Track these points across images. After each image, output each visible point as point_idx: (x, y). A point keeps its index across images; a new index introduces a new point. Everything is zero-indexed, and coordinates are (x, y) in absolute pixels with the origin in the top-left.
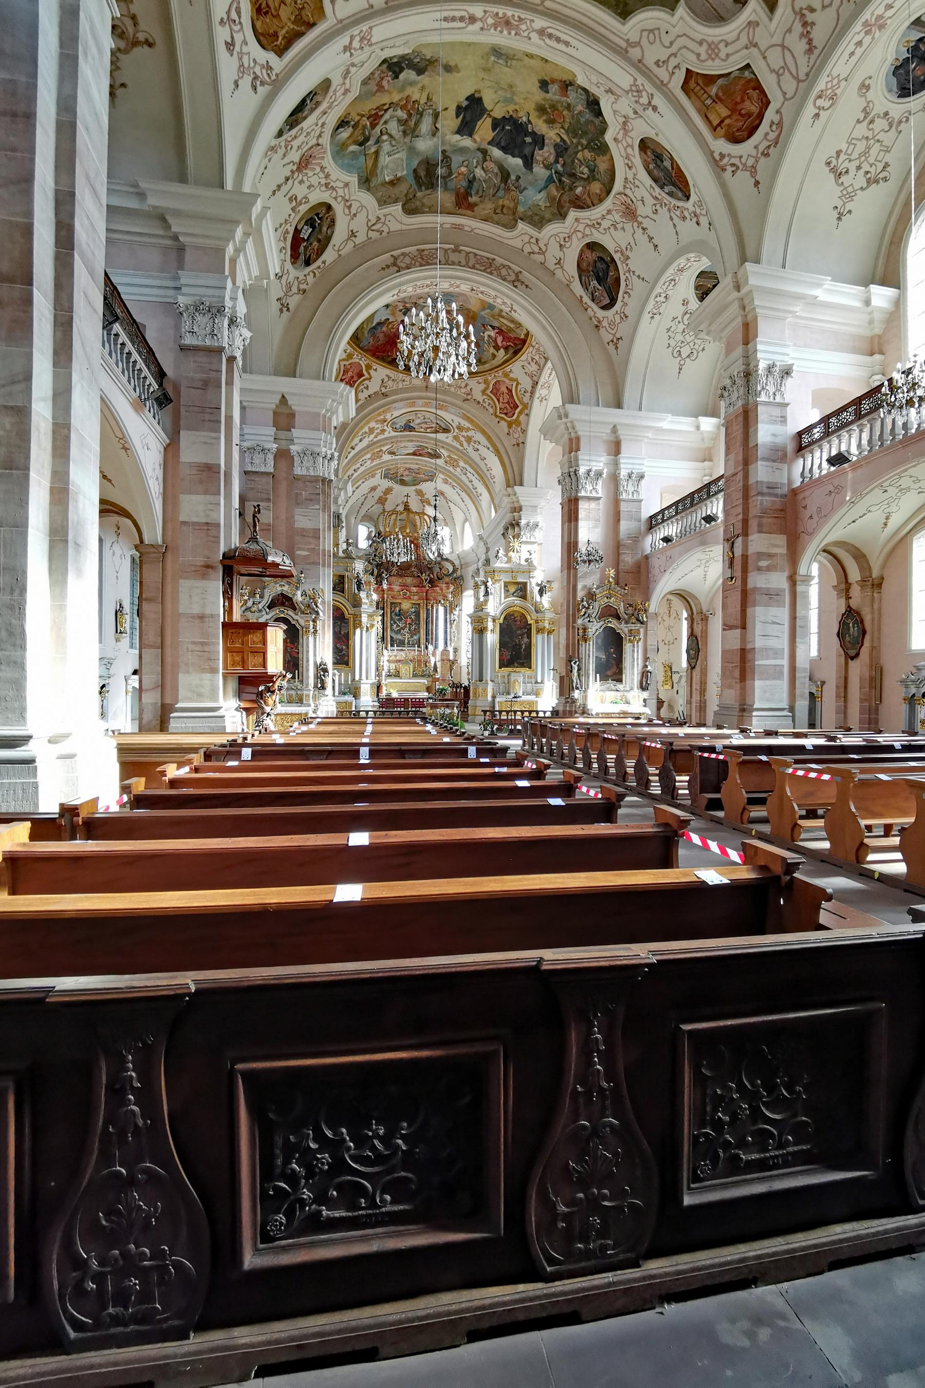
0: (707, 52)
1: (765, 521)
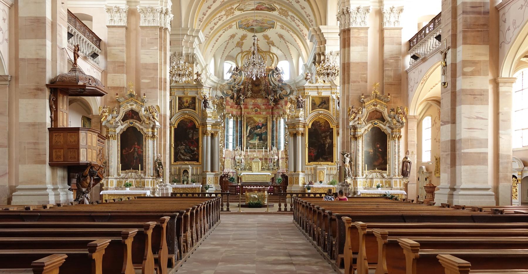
1: (469, 34)
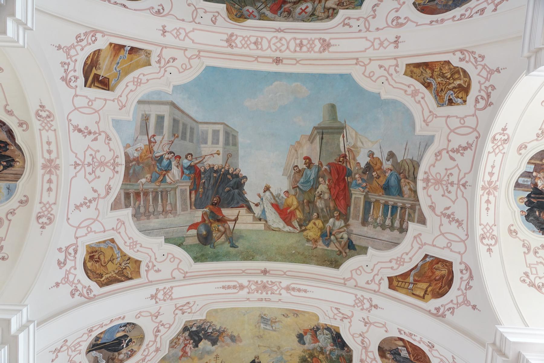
0: (396, 263)
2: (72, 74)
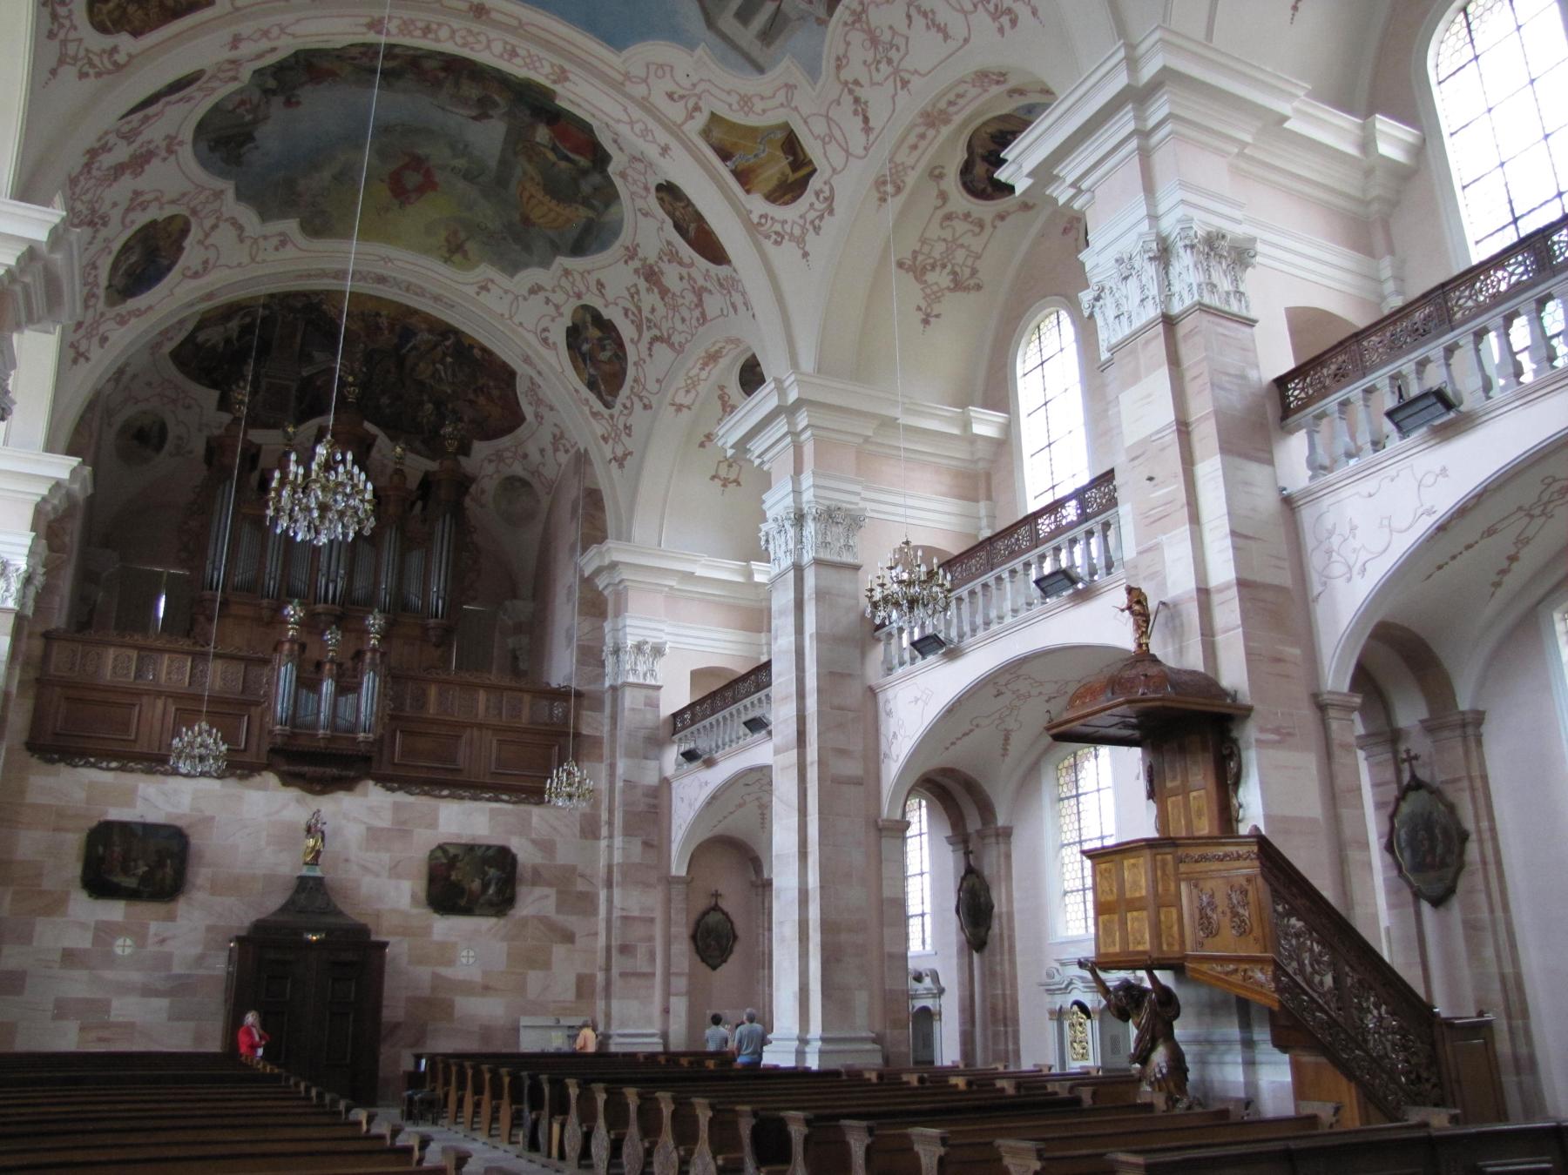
2: (819, 206)
